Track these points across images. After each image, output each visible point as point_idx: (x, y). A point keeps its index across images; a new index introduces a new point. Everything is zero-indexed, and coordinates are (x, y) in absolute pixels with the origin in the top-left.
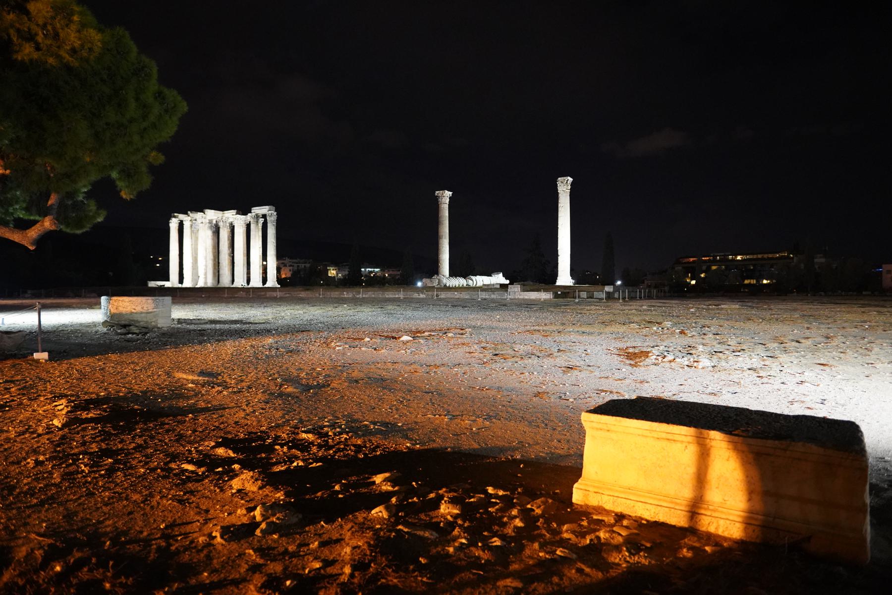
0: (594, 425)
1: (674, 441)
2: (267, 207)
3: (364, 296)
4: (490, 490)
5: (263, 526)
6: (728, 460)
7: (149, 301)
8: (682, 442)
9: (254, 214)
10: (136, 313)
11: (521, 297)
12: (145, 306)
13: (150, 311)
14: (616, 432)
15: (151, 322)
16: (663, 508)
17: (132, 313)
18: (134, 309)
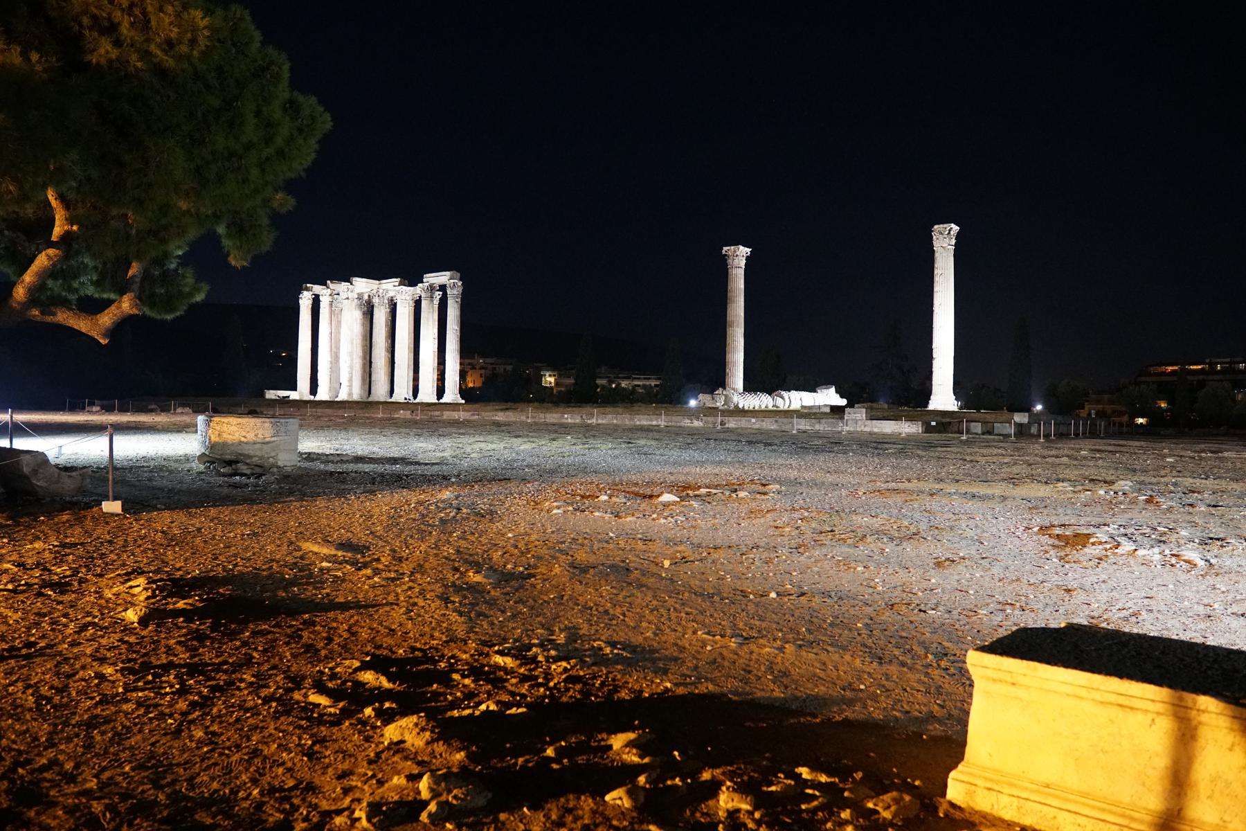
0: (990, 673)
1: (1132, 708)
2: (448, 273)
3: (600, 421)
4: (805, 772)
5: (432, 807)
6: (1231, 750)
7: (266, 425)
8: (1146, 711)
9: (427, 284)
10: (246, 443)
11: (867, 429)
12: (260, 432)
13: (267, 440)
14: (1028, 687)
15: (268, 458)
16: (1109, 825)
17: (241, 442)
18: (245, 437)
